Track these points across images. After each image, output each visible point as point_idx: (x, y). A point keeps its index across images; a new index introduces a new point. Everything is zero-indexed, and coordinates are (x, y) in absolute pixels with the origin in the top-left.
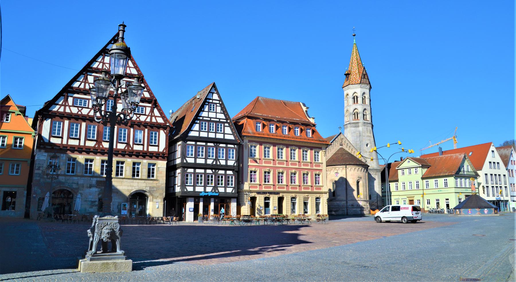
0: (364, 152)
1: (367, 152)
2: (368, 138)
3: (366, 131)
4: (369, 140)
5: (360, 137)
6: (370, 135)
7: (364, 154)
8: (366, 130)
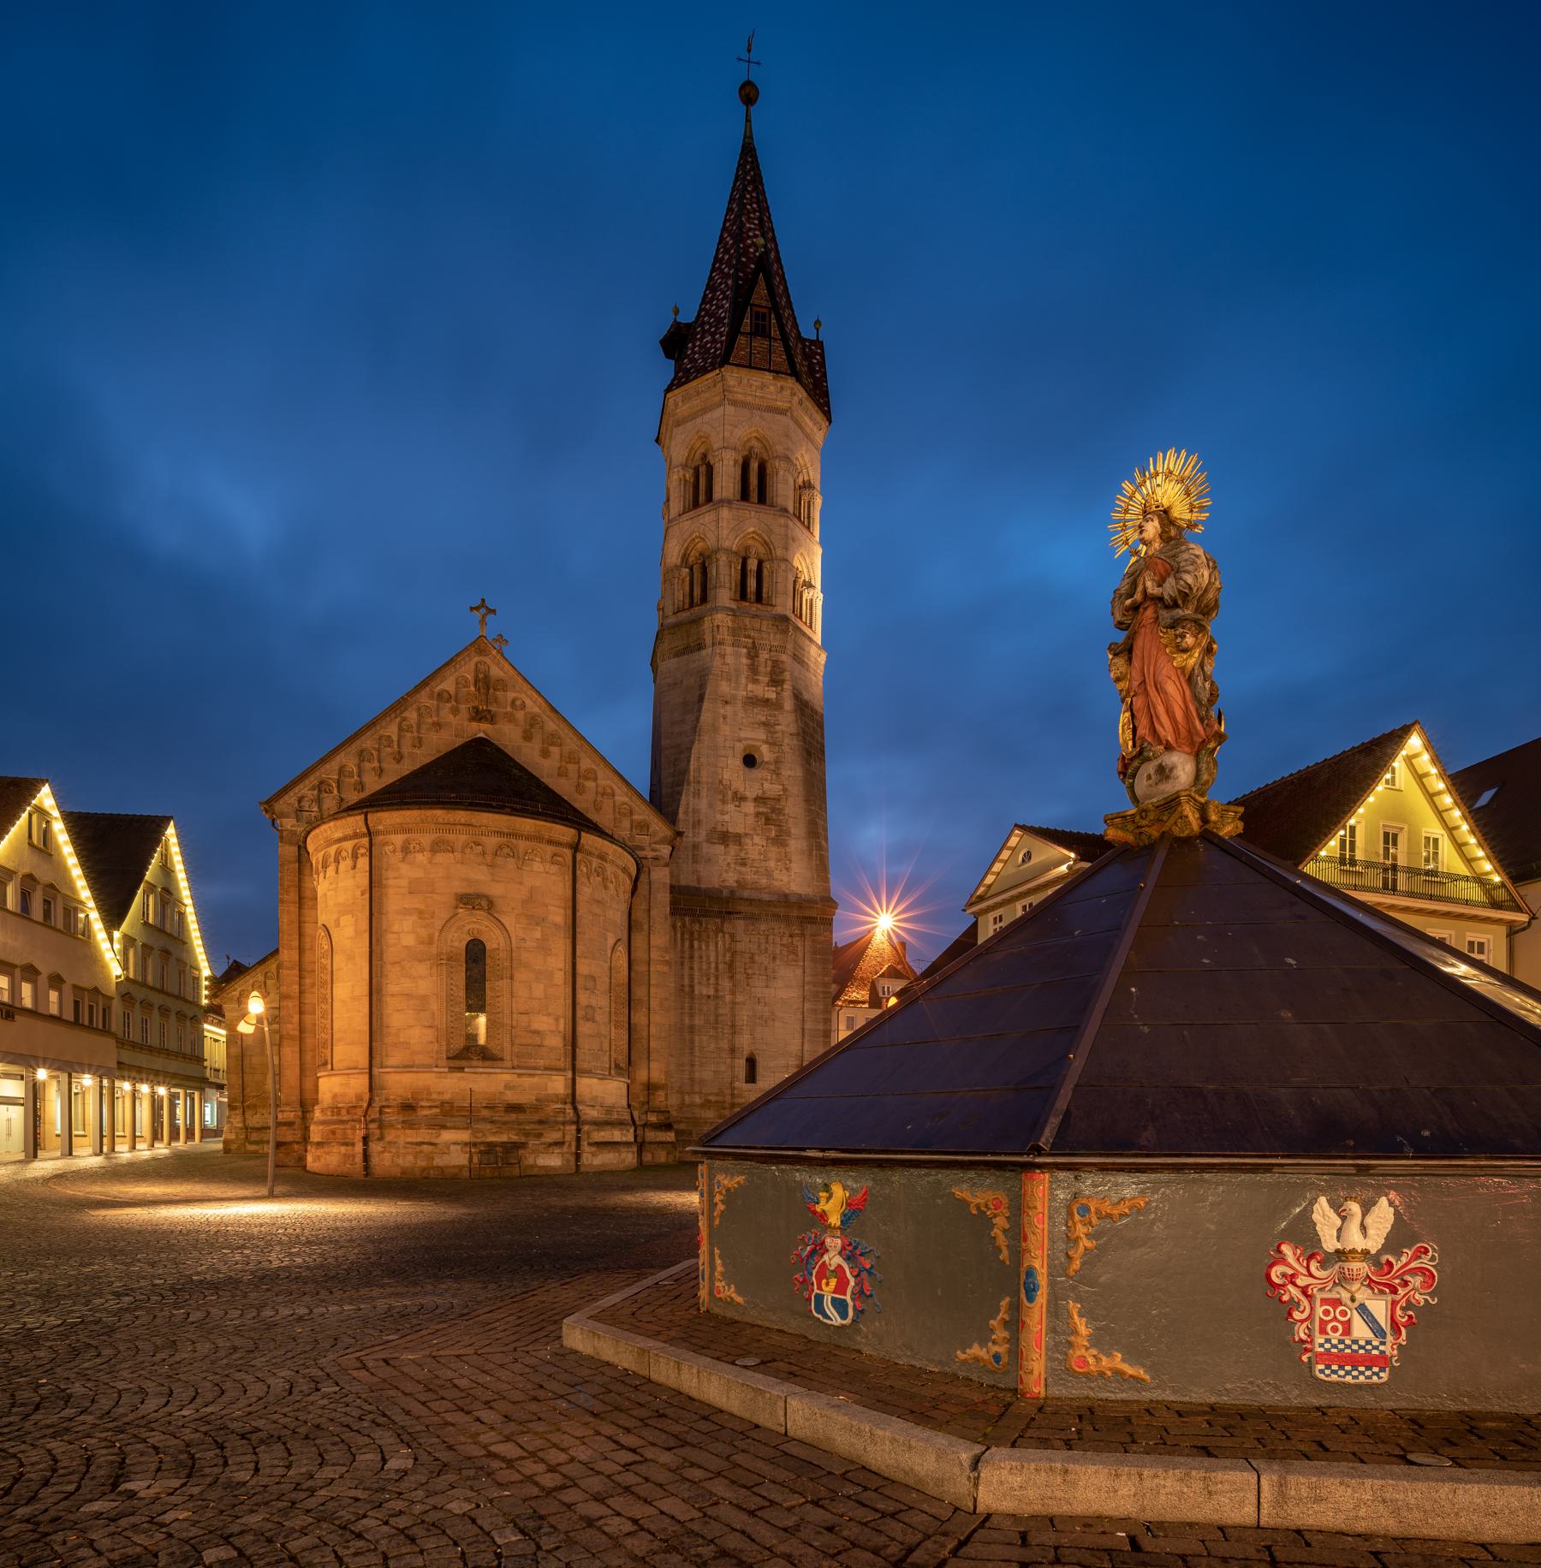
0: (724, 802)
1: (743, 799)
2: (761, 715)
3: (745, 672)
4: (765, 724)
5: (700, 710)
6: (773, 696)
7: (723, 813)
8: (745, 661)
